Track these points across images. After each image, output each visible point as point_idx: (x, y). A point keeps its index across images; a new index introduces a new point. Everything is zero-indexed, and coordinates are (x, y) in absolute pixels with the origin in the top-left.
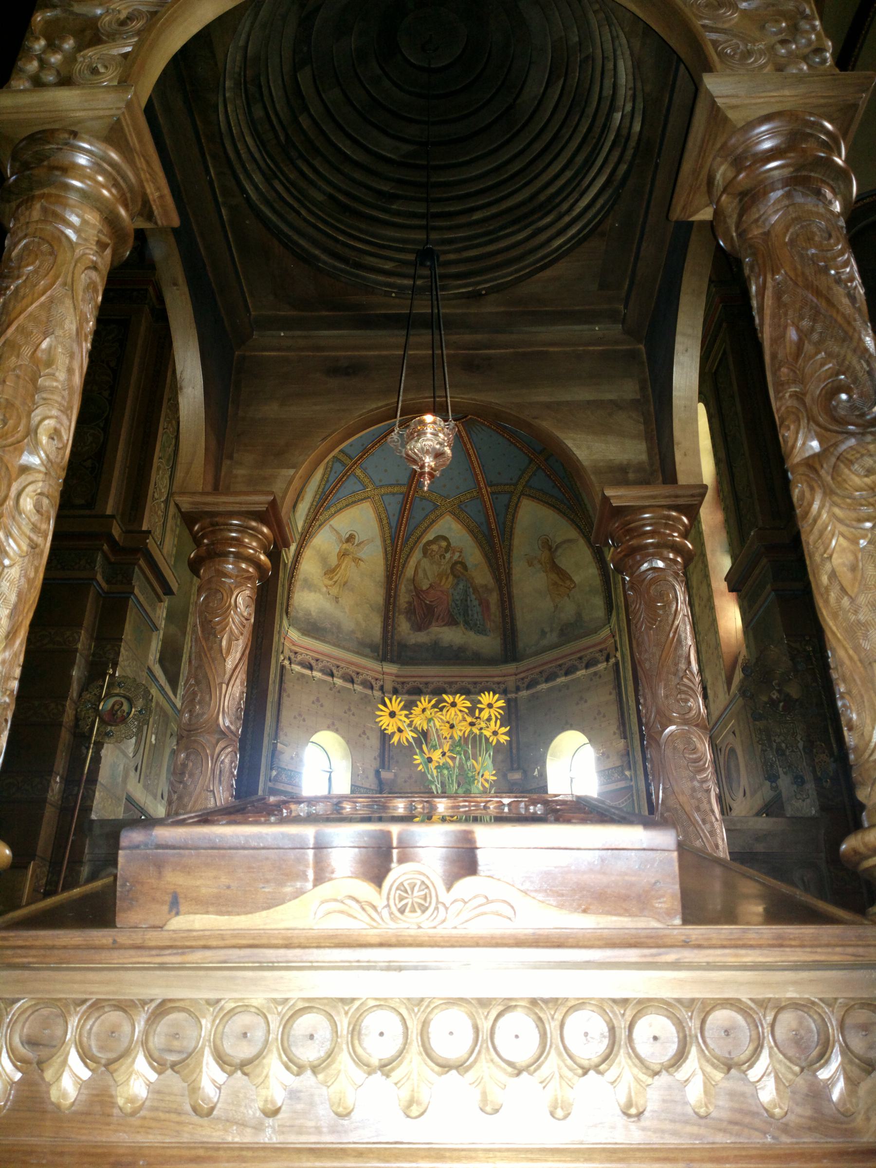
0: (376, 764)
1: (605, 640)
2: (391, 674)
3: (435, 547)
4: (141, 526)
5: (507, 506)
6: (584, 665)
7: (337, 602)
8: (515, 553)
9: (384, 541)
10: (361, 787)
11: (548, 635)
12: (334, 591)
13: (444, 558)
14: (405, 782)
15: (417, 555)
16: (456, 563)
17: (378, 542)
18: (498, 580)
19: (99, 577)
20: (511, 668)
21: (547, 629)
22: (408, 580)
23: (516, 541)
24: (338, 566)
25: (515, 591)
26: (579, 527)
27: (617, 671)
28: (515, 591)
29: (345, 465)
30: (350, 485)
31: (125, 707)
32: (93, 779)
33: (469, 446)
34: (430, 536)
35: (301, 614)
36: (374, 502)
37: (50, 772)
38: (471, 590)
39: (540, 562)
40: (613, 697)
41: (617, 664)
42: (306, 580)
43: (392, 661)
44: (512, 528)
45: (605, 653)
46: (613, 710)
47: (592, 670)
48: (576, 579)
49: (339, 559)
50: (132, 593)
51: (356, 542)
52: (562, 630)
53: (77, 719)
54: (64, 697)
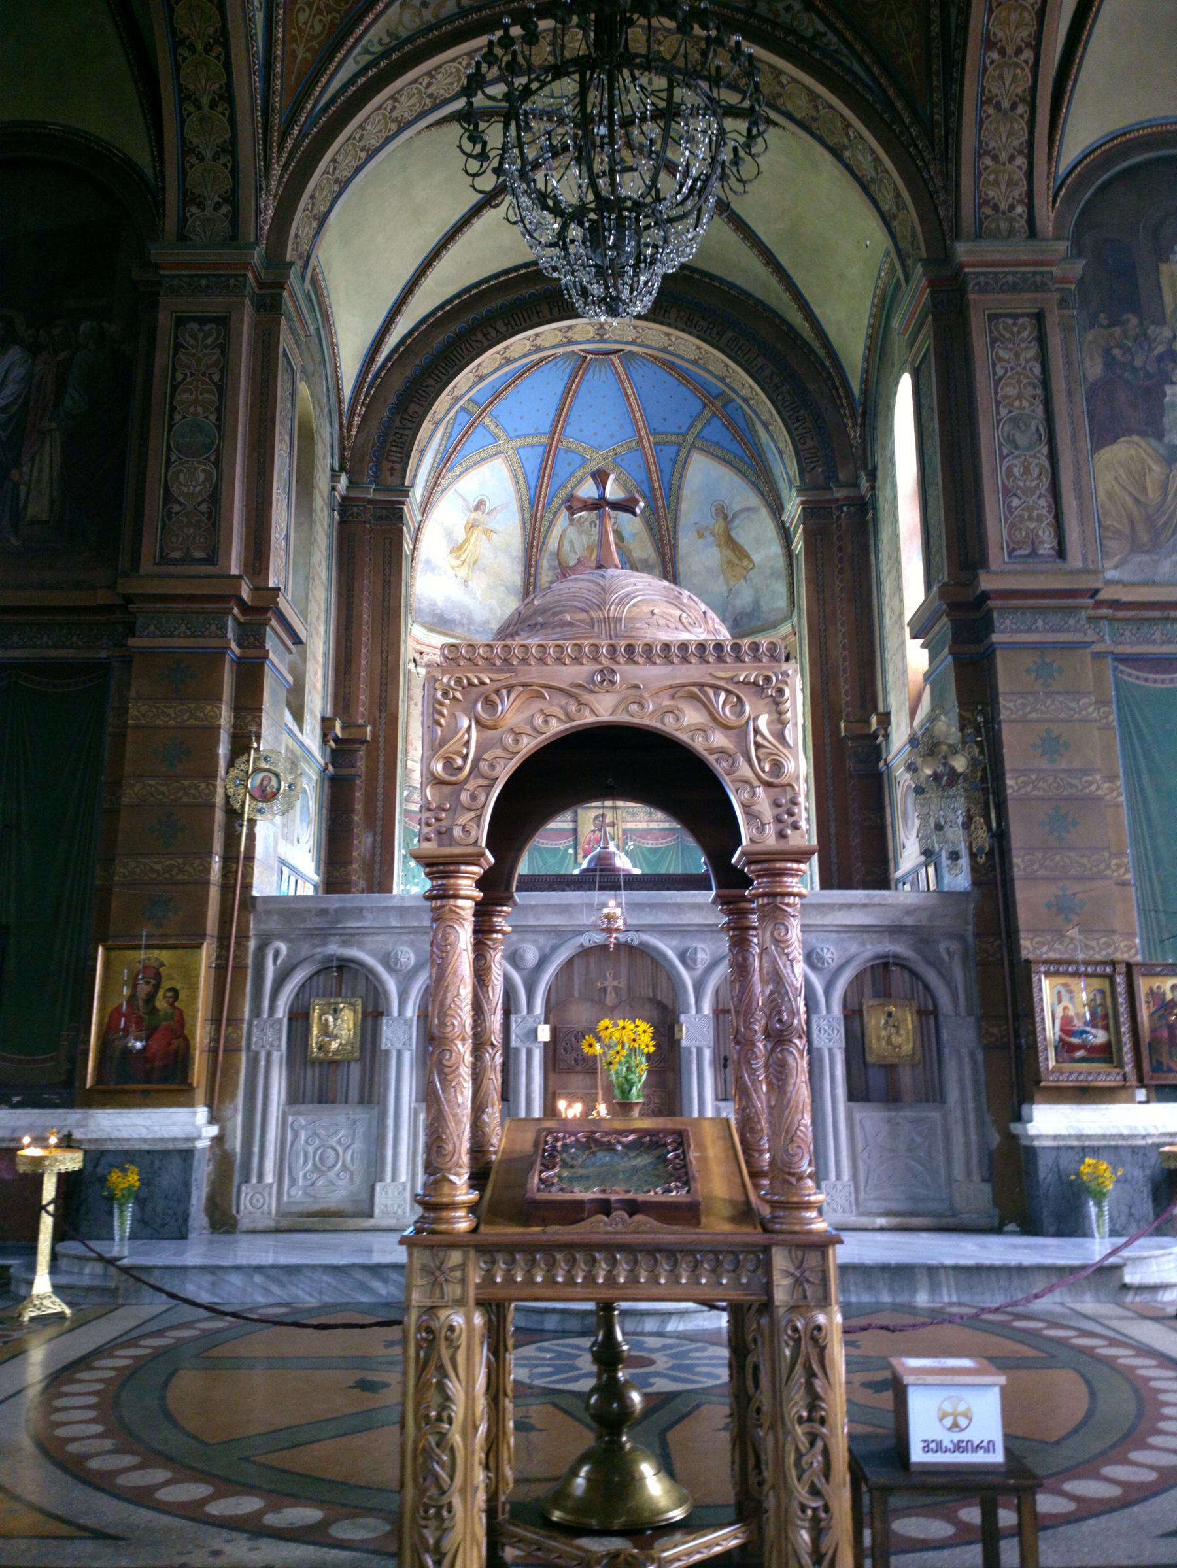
4: (267, 579)
5: (674, 461)
8: (683, 521)
9: (521, 505)
12: (463, 572)
17: (514, 508)
18: (661, 553)
19: (233, 645)
22: (551, 554)
23: (684, 506)
24: (466, 541)
29: (471, 414)
30: (478, 437)
31: (274, 783)
32: (250, 858)
33: (627, 385)
35: (424, 605)
36: (508, 459)
37: (210, 854)
42: (428, 562)
44: (679, 488)
48: (756, 557)
49: (467, 533)
50: (267, 658)
52: (735, 620)
53: (227, 797)
54: (215, 777)
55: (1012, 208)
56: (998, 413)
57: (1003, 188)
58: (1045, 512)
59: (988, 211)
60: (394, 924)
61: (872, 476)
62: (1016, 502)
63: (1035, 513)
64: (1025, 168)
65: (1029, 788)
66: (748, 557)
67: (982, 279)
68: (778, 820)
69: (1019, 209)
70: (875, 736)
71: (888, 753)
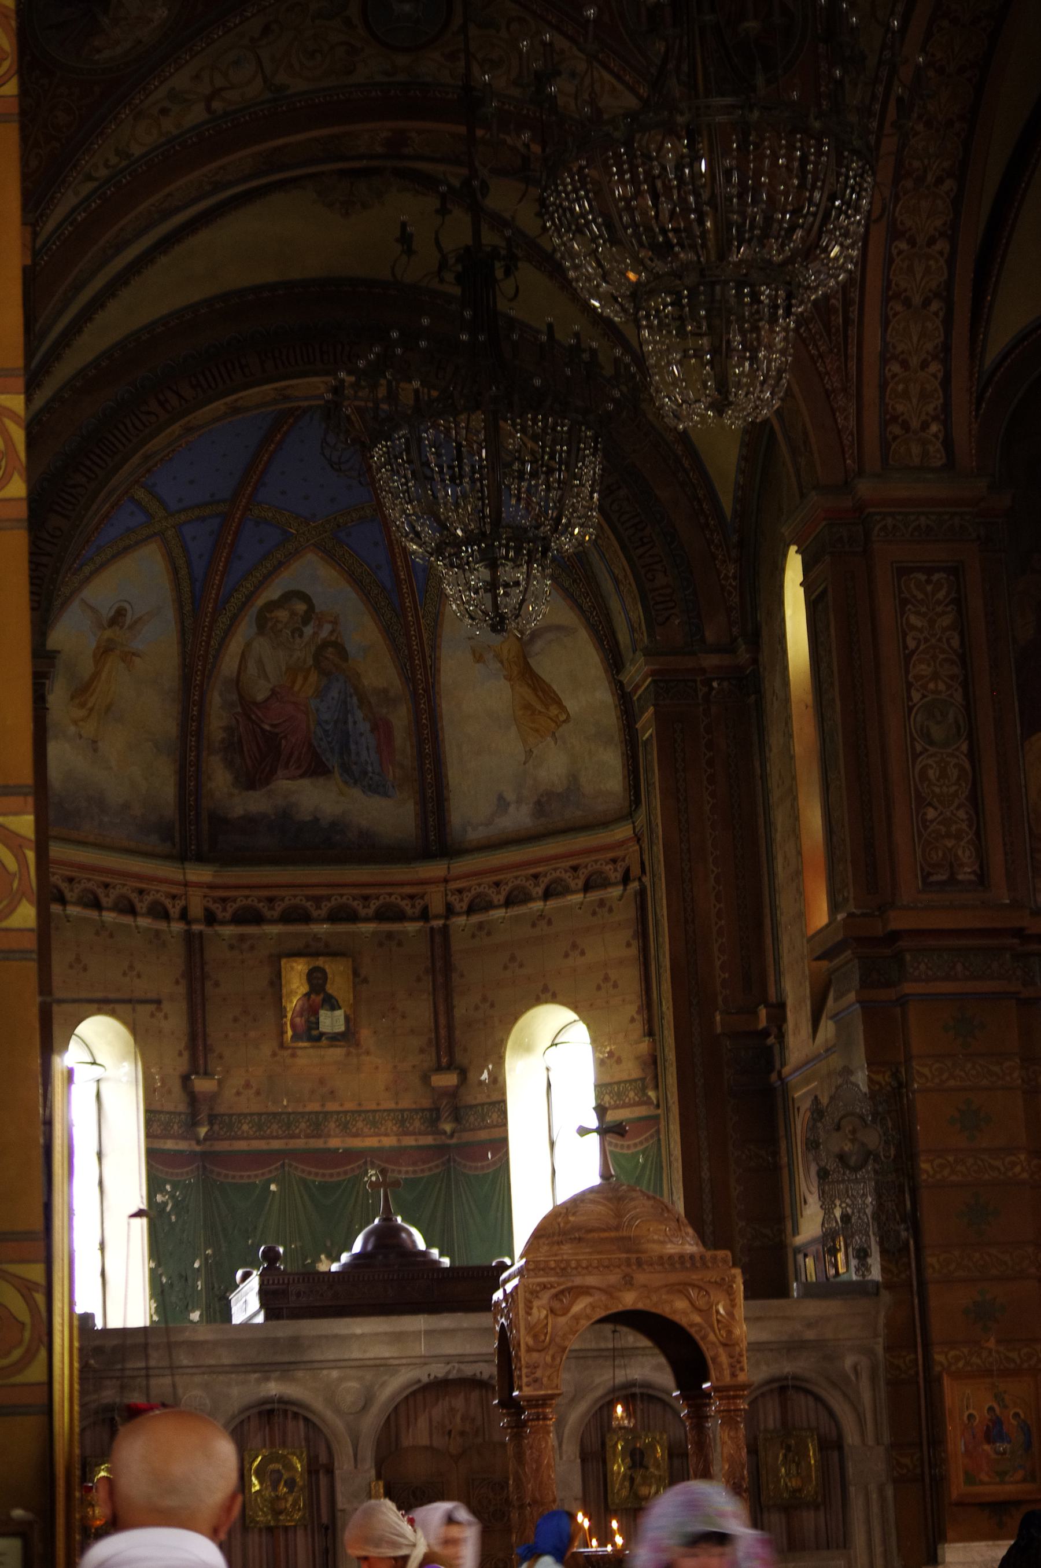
0: (182, 1064)
1: (622, 844)
2: (198, 885)
3: (282, 615)
6: (581, 883)
7: (95, 750)
10: (161, 1112)
11: (512, 809)
13: (301, 636)
14: (238, 1094)
15: (245, 630)
16: (325, 645)
17: (170, 613)
20: (435, 869)
21: (510, 796)
24: (95, 676)
25: (446, 707)
26: (580, 607)
27: (642, 908)
28: (443, 706)
34: (273, 592)
38: (355, 700)
39: (498, 657)
40: (634, 951)
41: (642, 893)
43: (201, 859)
45: (621, 867)
46: (630, 978)
47: (594, 896)
48: (571, 705)
51: (128, 622)
52: (538, 803)
55: (925, 426)
56: (910, 698)
57: (914, 401)
58: (964, 826)
59: (896, 430)
60: (185, 1362)
61: (754, 640)
62: (931, 814)
63: (954, 828)
64: (940, 375)
65: (946, 1172)
66: (559, 703)
67: (889, 521)
68: (732, 1366)
69: (934, 428)
70: (765, 1033)
71: (783, 1064)
